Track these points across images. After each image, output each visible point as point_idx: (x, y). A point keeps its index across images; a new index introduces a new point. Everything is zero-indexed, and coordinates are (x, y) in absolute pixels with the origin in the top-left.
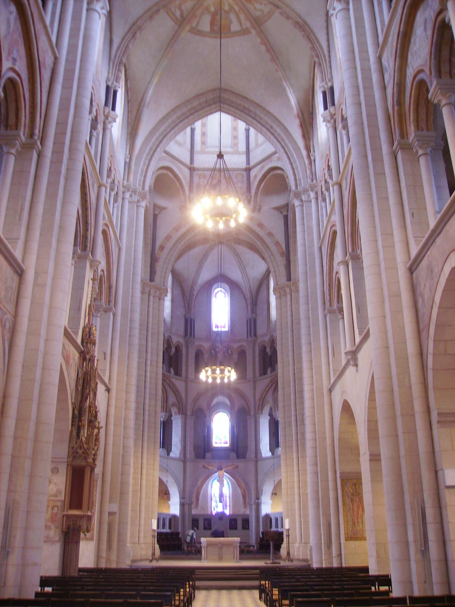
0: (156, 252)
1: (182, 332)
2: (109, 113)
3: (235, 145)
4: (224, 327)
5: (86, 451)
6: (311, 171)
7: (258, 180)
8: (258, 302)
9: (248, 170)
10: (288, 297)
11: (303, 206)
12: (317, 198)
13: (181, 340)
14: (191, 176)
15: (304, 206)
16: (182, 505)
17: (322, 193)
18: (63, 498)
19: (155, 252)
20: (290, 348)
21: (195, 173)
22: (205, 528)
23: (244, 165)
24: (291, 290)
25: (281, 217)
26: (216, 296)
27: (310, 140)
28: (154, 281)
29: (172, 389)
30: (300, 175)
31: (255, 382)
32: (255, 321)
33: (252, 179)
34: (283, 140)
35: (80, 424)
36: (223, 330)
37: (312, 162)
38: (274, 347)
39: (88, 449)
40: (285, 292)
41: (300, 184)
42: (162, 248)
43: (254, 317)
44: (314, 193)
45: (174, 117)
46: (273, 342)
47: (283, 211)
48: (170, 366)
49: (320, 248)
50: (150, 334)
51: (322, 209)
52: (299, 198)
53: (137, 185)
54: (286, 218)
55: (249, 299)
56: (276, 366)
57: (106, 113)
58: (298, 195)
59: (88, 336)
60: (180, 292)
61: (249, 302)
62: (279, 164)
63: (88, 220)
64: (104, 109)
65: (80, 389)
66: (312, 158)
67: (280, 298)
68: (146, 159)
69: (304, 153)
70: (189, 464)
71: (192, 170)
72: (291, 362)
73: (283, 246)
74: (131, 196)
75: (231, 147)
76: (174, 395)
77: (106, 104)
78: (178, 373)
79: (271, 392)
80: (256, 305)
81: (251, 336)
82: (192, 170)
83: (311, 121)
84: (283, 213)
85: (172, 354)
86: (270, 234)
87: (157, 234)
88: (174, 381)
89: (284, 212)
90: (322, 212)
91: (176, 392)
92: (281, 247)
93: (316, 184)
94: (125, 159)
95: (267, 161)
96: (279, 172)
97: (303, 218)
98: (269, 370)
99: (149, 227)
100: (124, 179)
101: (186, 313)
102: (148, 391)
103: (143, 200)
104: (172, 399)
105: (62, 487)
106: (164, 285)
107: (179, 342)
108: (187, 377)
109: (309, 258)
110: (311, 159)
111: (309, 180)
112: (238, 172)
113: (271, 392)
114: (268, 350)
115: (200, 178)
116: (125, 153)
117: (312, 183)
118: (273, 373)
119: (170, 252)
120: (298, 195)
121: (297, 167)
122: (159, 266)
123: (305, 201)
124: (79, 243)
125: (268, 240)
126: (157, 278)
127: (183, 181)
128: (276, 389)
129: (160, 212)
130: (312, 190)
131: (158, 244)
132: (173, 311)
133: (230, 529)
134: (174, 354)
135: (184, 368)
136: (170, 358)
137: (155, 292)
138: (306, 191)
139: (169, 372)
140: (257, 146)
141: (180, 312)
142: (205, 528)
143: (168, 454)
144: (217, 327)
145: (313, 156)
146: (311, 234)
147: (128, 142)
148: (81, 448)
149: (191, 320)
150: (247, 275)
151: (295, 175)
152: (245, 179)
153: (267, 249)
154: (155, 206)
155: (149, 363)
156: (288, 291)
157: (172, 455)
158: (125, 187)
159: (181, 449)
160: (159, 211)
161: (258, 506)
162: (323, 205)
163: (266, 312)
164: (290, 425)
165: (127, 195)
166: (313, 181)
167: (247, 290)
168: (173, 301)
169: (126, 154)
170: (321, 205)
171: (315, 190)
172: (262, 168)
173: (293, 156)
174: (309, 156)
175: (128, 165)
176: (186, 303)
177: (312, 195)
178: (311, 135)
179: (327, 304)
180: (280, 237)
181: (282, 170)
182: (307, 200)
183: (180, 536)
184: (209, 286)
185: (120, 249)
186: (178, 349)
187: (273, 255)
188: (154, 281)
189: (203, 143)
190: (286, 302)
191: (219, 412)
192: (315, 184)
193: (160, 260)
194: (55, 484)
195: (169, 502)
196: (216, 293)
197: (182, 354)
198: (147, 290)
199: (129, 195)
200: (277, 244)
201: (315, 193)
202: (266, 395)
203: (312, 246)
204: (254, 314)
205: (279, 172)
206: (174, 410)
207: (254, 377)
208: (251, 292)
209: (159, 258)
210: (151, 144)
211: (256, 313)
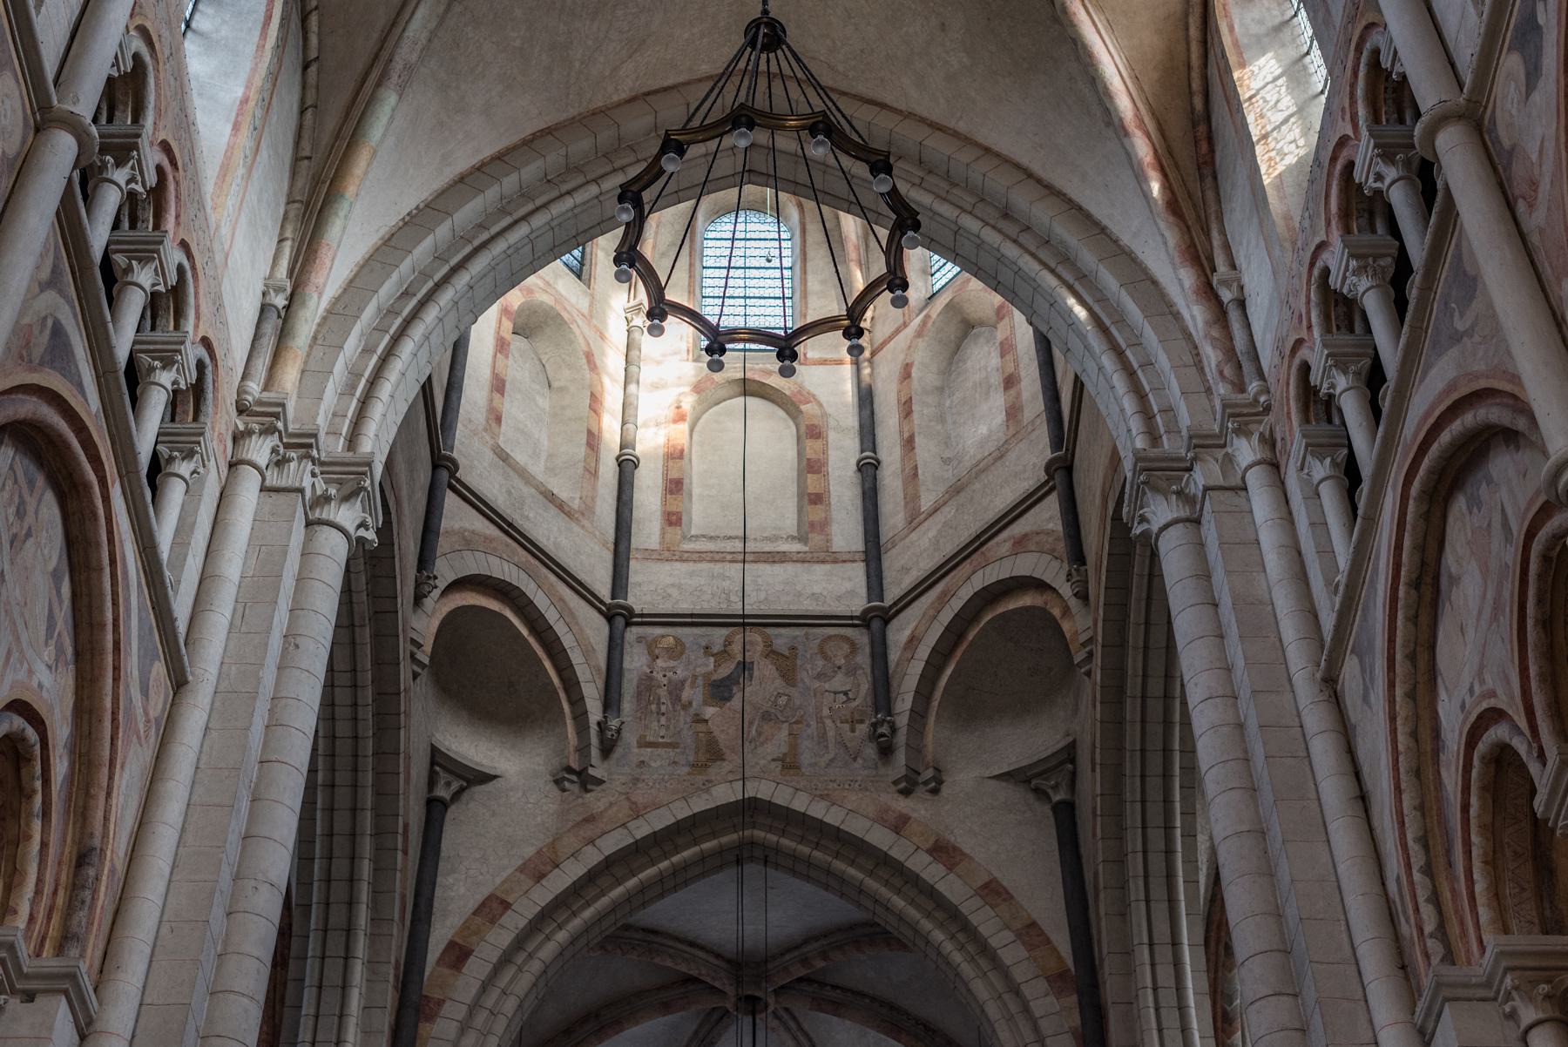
0: (427, 974)
3: (822, 526)
6: (1230, 353)
7: (924, 652)
9: (877, 619)
11: (1197, 522)
12: (1274, 466)
14: (615, 647)
15: (1207, 516)
17: (1308, 393)
21: (633, 633)
23: (858, 603)
33: (894, 656)
34: (1067, 259)
41: (1173, 429)
45: (531, 171)
49: (1330, 683)
53: (322, 421)
54: (1066, 817)
62: (1025, 565)
66: (1226, 295)
71: (618, 616)
73: (1062, 942)
75: (802, 538)
82: (618, 616)
83: (1204, 147)
84: (1049, 798)
89: (1055, 787)
93: (1262, 399)
95: (966, 568)
96: (1027, 600)
99: (400, 839)
103: (346, 498)
111: (1222, 389)
121: (1148, 364)
123: (1206, 489)
127: (576, 658)
130: (1242, 431)
131: (440, 935)
140: (915, 519)
145: (1229, 286)
147: (288, 234)
152: (864, 659)
154: (438, 760)
160: (455, 786)
166: (1241, 388)
172: (943, 600)
174: (1208, 291)
177: (1246, 451)
181: (1040, 585)
182: (1221, 482)
185: (179, 681)
189: (673, 519)
192: (1256, 400)
193: (447, 1009)
201: (1262, 438)
205: (1027, 600)
209: (440, 1003)
210: (406, 266)
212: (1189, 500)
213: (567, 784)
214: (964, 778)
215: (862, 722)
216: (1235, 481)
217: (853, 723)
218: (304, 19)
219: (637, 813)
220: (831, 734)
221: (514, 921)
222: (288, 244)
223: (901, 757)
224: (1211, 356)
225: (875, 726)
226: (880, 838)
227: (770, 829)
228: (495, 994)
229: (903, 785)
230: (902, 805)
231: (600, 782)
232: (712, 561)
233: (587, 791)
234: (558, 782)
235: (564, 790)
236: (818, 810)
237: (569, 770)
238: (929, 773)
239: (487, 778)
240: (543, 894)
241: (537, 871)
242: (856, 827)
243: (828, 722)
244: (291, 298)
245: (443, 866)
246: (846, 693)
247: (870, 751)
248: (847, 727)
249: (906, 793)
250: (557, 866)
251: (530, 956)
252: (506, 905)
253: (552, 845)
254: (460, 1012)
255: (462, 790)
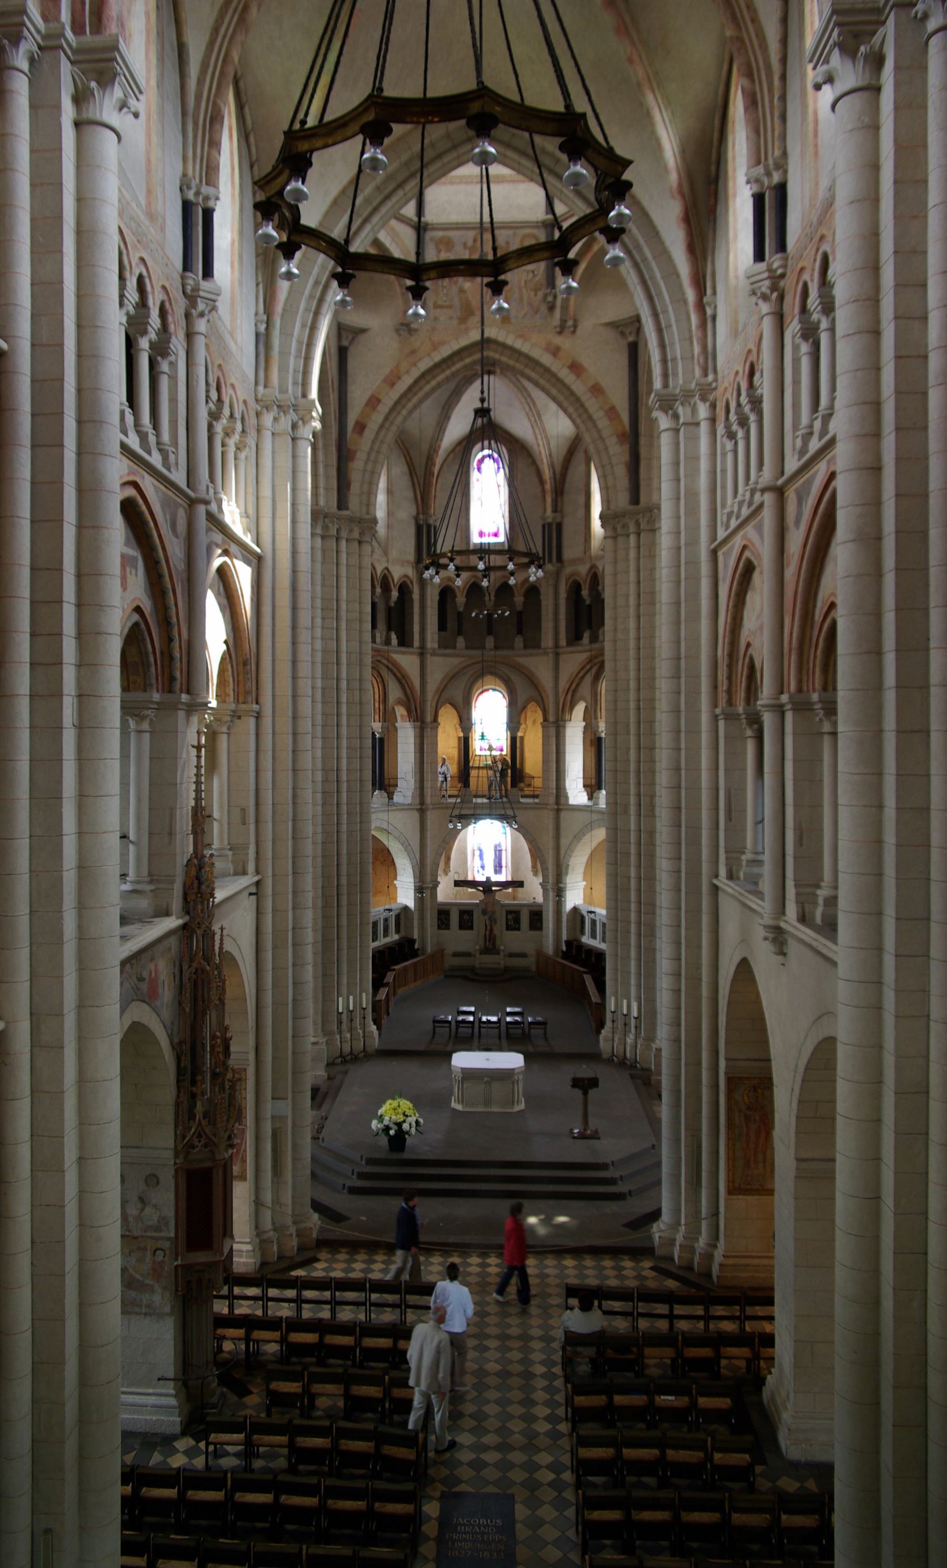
1: (411, 556)
2: (196, 289)
4: (496, 535)
5: (210, 1139)
8: (567, 486)
10: (632, 538)
12: (713, 420)
13: (410, 572)
16: (419, 890)
18: (172, 1235)
19: (346, 438)
20: (632, 653)
22: (461, 927)
24: (638, 524)
25: (623, 344)
26: (479, 469)
27: (705, 258)
28: (347, 508)
29: (394, 674)
30: (677, 350)
31: (557, 655)
32: (559, 527)
34: (638, 247)
35: (194, 1089)
36: (493, 540)
37: (707, 320)
38: (598, 591)
39: (215, 1135)
40: (625, 526)
42: (361, 427)
43: (558, 520)
44: (708, 404)
46: (595, 579)
47: (628, 331)
48: (389, 629)
50: (343, 625)
51: (724, 454)
52: (670, 412)
55: (548, 481)
56: (601, 632)
57: (189, 288)
58: (667, 404)
59: (196, 885)
60: (406, 469)
61: (548, 487)
63: (171, 618)
64: (183, 278)
65: (188, 1010)
66: (709, 312)
67: (615, 538)
68: (307, 310)
69: (690, 295)
70: (431, 816)
72: (632, 684)
74: (276, 419)
76: (397, 684)
77: (187, 265)
78: (405, 641)
79: (589, 679)
80: (562, 493)
81: (550, 561)
85: (393, 605)
86: (597, 390)
87: (349, 395)
88: (398, 657)
89: (630, 333)
90: (724, 462)
91: (402, 679)
92: (621, 421)
94: (256, 325)
97: (677, 463)
98: (586, 635)
100: (256, 383)
101: (418, 513)
102: (344, 743)
104: (395, 692)
105: (170, 1213)
106: (368, 513)
107: (406, 576)
108: (423, 646)
109: (686, 571)
110: (704, 313)
111: (698, 372)
112: (527, 231)
113: (589, 679)
114: (585, 593)
115: (439, 251)
116: (253, 312)
117: (703, 380)
118: (595, 646)
119: (378, 433)
120: (667, 404)
121: (669, 326)
122: (357, 468)
124: (154, 681)
125: (592, 405)
126: (354, 501)
128: (597, 678)
129: (351, 343)
131: (352, 417)
132: (390, 514)
133: (508, 928)
134: (395, 603)
135: (416, 628)
136: (389, 610)
137: (351, 531)
138: (687, 396)
139: (388, 642)
141: (407, 511)
142: (461, 927)
143: (390, 796)
144: (481, 534)
146: (693, 510)
148: (200, 1136)
149: (429, 527)
150: (544, 430)
151: (662, 346)
153: (590, 424)
155: (344, 685)
156: (632, 528)
157: (397, 798)
158: (261, 401)
159: (415, 788)
160: (350, 337)
161: (560, 893)
162: (729, 446)
163: (582, 511)
164: (626, 811)
165: (268, 419)
167: (545, 461)
168: (390, 492)
169: (256, 314)
170: (723, 446)
171: (711, 398)
173: (660, 294)
174: (701, 306)
175: (263, 340)
176: (418, 492)
178: (710, 245)
179: (722, 697)
180: (619, 397)
182: (689, 420)
183: (416, 946)
184: (465, 447)
186: (404, 589)
187: (602, 439)
188: (347, 508)
190: (627, 549)
191: (487, 690)
193: (359, 455)
194: (155, 1206)
195: (395, 882)
196: (481, 461)
197: (412, 600)
198: (333, 532)
199: (272, 419)
200: (611, 412)
202: (578, 685)
203: (693, 541)
204: (558, 515)
206: (400, 711)
207: (557, 646)
208: (552, 466)
209: (355, 452)
211: (561, 511)
212: (676, 417)
213: (402, 333)
214: (588, 324)
215: (540, 290)
216: (695, 421)
217: (536, 291)
218: (247, 138)
219: (435, 347)
220: (525, 298)
221: (383, 409)
222: (261, 286)
223: (557, 313)
224: (697, 349)
225: (546, 296)
226: (546, 359)
227: (496, 351)
228: (378, 444)
229: (558, 330)
230: (558, 340)
231: (416, 330)
232: (467, 183)
233: (411, 335)
234: (397, 331)
235: (400, 335)
236: (518, 345)
237: (402, 324)
238: (570, 323)
239: (363, 331)
240: (395, 394)
241: (391, 380)
242: (537, 354)
243: (524, 291)
244: (268, 323)
245: (350, 380)
246: (533, 272)
247: (544, 309)
248: (532, 294)
249: (560, 333)
250: (399, 378)
251: (392, 423)
252: (379, 401)
253: (397, 367)
254: (364, 456)
255: (353, 339)
